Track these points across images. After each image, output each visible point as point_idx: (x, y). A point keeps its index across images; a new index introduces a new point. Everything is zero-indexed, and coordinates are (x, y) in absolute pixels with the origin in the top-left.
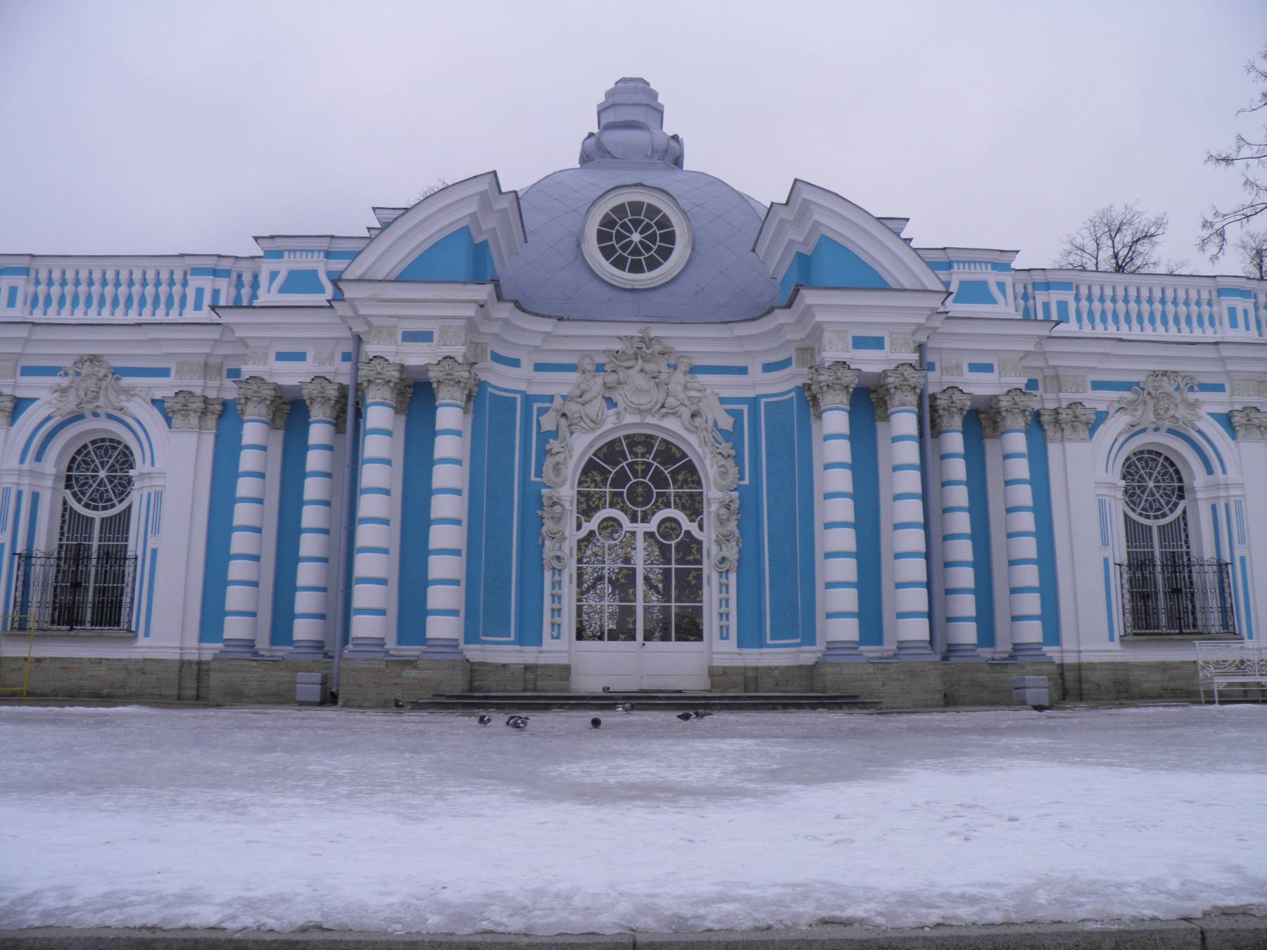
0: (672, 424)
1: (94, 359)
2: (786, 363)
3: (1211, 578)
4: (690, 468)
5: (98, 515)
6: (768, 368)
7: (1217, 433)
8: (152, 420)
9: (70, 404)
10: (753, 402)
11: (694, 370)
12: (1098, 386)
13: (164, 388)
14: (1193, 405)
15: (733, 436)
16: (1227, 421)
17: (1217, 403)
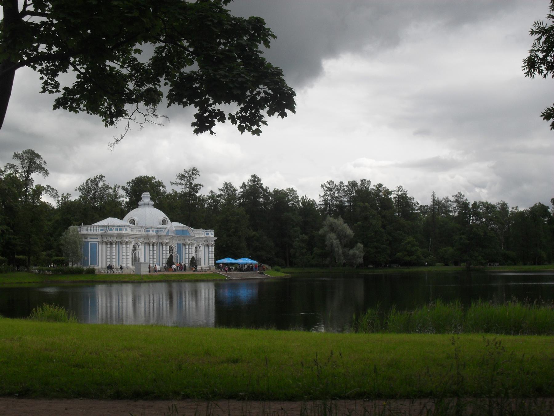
0: (173, 245)
1: (136, 237)
2: (181, 240)
3: (199, 259)
4: (172, 249)
5: (134, 253)
6: (179, 240)
7: (201, 245)
8: (140, 244)
9: (135, 242)
10: (177, 243)
11: (174, 240)
12: (195, 241)
13: (141, 240)
14: (200, 243)
15: (176, 246)
16: (202, 244)
17: (201, 243)
